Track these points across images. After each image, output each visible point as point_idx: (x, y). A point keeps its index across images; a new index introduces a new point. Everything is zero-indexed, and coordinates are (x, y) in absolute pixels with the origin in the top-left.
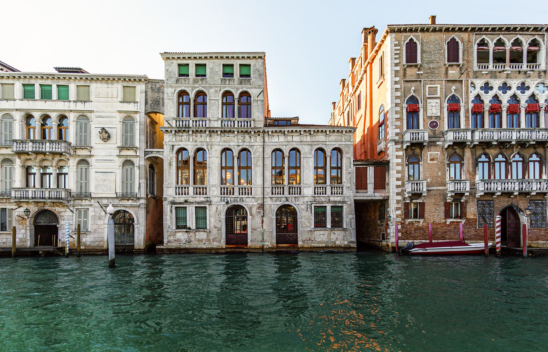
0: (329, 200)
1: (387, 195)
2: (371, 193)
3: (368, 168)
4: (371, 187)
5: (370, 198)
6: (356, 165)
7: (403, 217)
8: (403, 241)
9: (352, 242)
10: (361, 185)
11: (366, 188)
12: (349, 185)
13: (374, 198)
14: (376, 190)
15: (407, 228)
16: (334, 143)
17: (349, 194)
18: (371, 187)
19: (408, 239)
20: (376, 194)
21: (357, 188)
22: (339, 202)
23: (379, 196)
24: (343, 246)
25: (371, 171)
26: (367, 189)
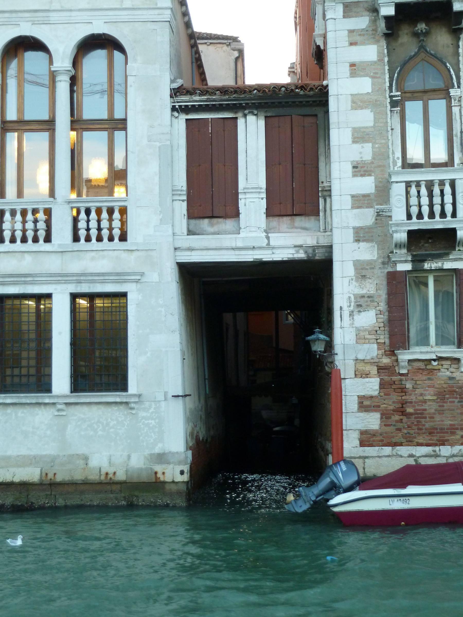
1: (324, 242)
3: (241, 122)
6: (186, 110)
8: (388, 450)
13: (267, 256)
14: (275, 222)
15: (403, 390)
19: (410, 441)
20: (277, 239)
21: (194, 213)
23: (285, 244)
24: (121, 476)
25: (252, 134)
26: (236, 215)
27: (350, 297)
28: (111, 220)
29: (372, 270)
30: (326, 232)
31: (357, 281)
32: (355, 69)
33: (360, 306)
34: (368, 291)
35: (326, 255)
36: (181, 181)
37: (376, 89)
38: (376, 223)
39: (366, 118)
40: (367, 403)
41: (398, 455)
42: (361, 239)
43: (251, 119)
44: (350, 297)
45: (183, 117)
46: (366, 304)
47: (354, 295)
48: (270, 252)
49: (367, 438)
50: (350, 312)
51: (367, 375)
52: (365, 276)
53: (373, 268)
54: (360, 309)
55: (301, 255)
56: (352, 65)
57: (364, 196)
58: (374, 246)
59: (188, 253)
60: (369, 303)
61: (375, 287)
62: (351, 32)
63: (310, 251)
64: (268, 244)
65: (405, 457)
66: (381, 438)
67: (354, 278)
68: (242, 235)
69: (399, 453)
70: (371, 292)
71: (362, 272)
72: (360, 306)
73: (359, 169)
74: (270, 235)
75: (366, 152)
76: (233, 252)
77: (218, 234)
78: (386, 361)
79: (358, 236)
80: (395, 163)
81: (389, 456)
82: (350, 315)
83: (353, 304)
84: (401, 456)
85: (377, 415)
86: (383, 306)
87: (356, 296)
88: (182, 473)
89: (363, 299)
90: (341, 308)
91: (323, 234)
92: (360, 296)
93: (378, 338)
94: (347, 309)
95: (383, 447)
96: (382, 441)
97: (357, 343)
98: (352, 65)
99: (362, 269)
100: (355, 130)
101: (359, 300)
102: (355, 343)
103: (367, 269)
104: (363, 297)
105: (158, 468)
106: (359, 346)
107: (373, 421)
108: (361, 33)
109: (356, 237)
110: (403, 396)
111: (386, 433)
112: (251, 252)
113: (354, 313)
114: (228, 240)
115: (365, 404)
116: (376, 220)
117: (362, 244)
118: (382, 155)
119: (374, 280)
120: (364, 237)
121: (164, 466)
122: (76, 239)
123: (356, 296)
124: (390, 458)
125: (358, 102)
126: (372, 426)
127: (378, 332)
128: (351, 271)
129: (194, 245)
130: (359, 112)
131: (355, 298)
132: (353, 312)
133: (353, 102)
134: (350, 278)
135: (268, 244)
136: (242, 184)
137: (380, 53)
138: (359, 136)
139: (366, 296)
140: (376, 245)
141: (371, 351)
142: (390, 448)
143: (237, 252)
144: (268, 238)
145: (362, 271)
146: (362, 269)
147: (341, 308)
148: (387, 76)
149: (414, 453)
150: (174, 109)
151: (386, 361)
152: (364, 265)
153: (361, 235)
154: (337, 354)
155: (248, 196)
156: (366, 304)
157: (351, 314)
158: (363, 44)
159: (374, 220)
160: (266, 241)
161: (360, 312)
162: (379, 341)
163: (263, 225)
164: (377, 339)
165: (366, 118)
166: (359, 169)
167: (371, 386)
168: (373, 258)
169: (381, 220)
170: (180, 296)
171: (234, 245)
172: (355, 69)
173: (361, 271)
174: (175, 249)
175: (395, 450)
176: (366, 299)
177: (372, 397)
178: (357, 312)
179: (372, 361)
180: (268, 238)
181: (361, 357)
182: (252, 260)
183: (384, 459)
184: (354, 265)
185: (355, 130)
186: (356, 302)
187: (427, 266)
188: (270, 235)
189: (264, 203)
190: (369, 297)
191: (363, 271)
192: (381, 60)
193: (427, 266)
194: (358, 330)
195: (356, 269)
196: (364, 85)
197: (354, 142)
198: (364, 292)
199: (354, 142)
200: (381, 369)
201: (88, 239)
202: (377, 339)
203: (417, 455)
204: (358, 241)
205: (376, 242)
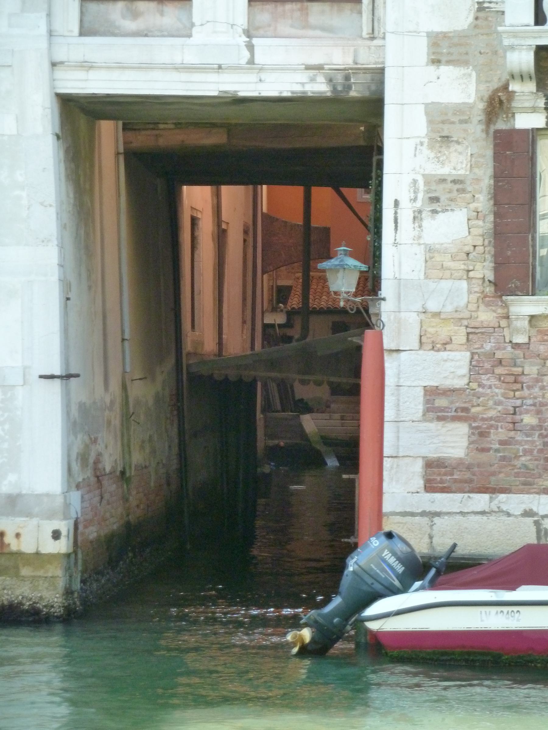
1: (368, 59)
5: (208, 86)
7: (485, 270)
8: (481, 501)
13: (247, 86)
20: (268, 50)
27: (415, 182)
29: (464, 126)
30: (373, 38)
31: (431, 147)
33: (435, 200)
34: (455, 169)
35: (373, 88)
38: (476, 26)
40: (442, 402)
41: (503, 511)
42: (444, 59)
44: (415, 182)
46: (448, 196)
47: (423, 175)
48: (252, 77)
49: (439, 476)
50: (414, 212)
51: (446, 345)
52: (447, 137)
53: (466, 122)
54: (435, 206)
55: (320, 87)
58: (470, 75)
59: (81, 74)
60: (455, 194)
61: (470, 160)
63: (339, 78)
64: (251, 62)
65: (516, 516)
66: (468, 475)
67: (426, 140)
69: (504, 508)
70: (460, 172)
71: (443, 129)
72: (435, 200)
74: (255, 41)
76: (175, 76)
77: (146, 35)
78: (486, 316)
79: (438, 53)
81: (483, 513)
82: (414, 218)
83: (420, 196)
84: (509, 515)
86: (483, 202)
87: (428, 179)
88: (56, 535)
89: (442, 186)
90: (397, 203)
91: (368, 43)
92: (439, 177)
93: (471, 268)
94: (410, 205)
95: (471, 495)
96: (471, 481)
97: (427, 277)
99: (443, 122)
101: (433, 188)
102: (422, 276)
103: (453, 123)
104: (443, 180)
106: (432, 285)
107: (453, 442)
109: (434, 53)
110: (518, 390)
111: (479, 465)
112: (213, 77)
113: (424, 215)
114: (165, 50)
115: (440, 404)
116: (477, 18)
117: (444, 69)
119: (467, 147)
120: (449, 53)
121: (20, 520)
123: (428, 179)
124: (485, 518)
126: (452, 451)
127: (471, 256)
128: (419, 126)
129: (93, 57)
131: (427, 183)
132: (420, 212)
134: (418, 141)
135: (251, 62)
139: (450, 179)
140: (474, 74)
141: (456, 294)
142: (486, 496)
143: (184, 76)
144: (250, 47)
145: (442, 128)
146: (443, 122)
147: (397, 203)
149: (535, 509)
151: (486, 316)
152: (446, 114)
153: (444, 50)
154: (384, 299)
156: (448, 196)
157: (417, 217)
159: (471, 18)
160: (246, 54)
161: (435, 212)
162: (471, 274)
163: (242, 20)
164: (468, 271)
167: (452, 368)
168: (467, 101)
169: (486, 19)
170: (62, 165)
171: (178, 60)
173: (441, 125)
174: (54, 65)
175: (496, 502)
176: (449, 186)
177: (453, 391)
178: (430, 213)
179: (457, 315)
180: (250, 47)
181: (433, 306)
182: (215, 94)
183: (472, 518)
184: (427, 114)
186: (427, 192)
188: (255, 41)
190: (454, 182)
191: (446, 127)
194: (431, 251)
195: (430, 122)
198: (445, 170)
200: (473, 333)
202: (468, 271)
203: (541, 513)
204: (436, 62)
205: (475, 67)
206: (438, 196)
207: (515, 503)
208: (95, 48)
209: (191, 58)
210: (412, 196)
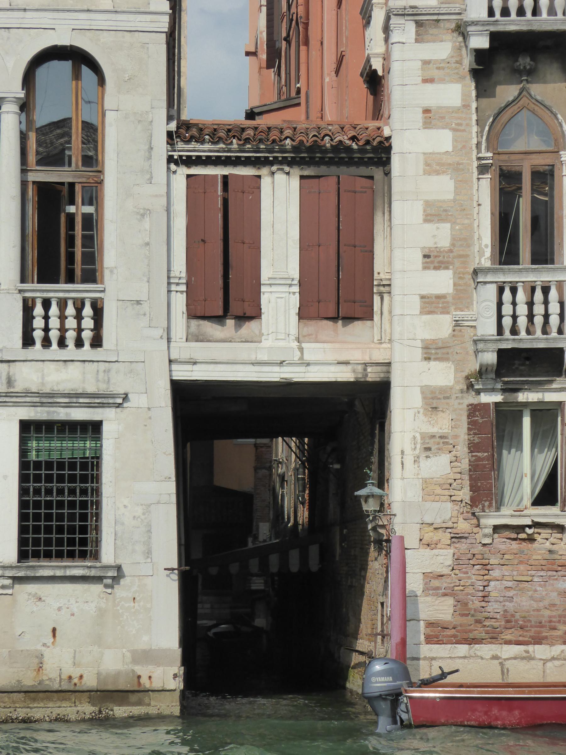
0: (10, 382)
1: (379, 356)
2: (280, 348)
3: (266, 182)
4: (280, 301)
5: (273, 375)
6: (189, 162)
8: (463, 649)
9: (146, 656)
10: (223, 289)
11: (250, 314)
12: (140, 290)
14: (312, 327)
16: (46, 19)
17: (143, 350)
18: (280, 301)
20: (313, 351)
22: (74, 398)
25: (280, 199)
27: (414, 438)
28: (79, 317)
29: (448, 401)
30: (381, 343)
31: (425, 415)
32: (430, 117)
33: (429, 449)
34: (441, 429)
35: (382, 375)
36: (180, 266)
37: (460, 146)
38: (454, 336)
39: (443, 187)
41: (478, 656)
42: (432, 357)
43: (280, 177)
44: (414, 438)
45: (183, 171)
46: (437, 446)
47: (420, 433)
48: (302, 369)
50: (414, 457)
52: (436, 408)
53: (448, 398)
54: (428, 453)
56: (427, 111)
57: (438, 297)
58: (450, 367)
59: (189, 367)
60: (441, 445)
61: (452, 423)
62: (426, 63)
64: (302, 358)
65: (487, 659)
66: (453, 632)
67: (422, 411)
68: (266, 343)
69: (479, 653)
70: (444, 431)
71: (433, 403)
72: (429, 449)
73: (432, 259)
74: (304, 345)
75: (441, 236)
76: (251, 368)
77: (230, 341)
78: (463, 526)
79: (429, 353)
80: (481, 253)
81: (465, 657)
82: (415, 461)
83: (418, 446)
84: (482, 658)
85: (450, 601)
89: (433, 440)
90: (403, 452)
91: (378, 346)
92: (431, 434)
93: (453, 494)
94: (411, 453)
95: (456, 645)
96: (455, 636)
97: (424, 500)
98: (427, 111)
99: (433, 398)
100: (428, 204)
101: (427, 441)
102: (421, 499)
103: (439, 399)
104: (433, 436)
105: (143, 671)
106: (428, 505)
108: (440, 65)
109: (426, 353)
110: (486, 575)
111: (461, 625)
112: (277, 369)
113: (421, 459)
116: (454, 331)
117: (432, 363)
118: (463, 240)
119: (449, 414)
120: (436, 353)
121: (150, 667)
122: (28, 341)
124: (466, 661)
125: (433, 165)
126: (443, 616)
127: (453, 487)
128: (417, 401)
129: (198, 356)
130: (435, 178)
131: (423, 438)
132: (418, 457)
133: (427, 164)
134: (416, 410)
135: (302, 358)
136: (266, 273)
137: (465, 96)
138: (434, 213)
139: (438, 435)
140: (453, 367)
141: (444, 511)
142: (466, 646)
143: (257, 368)
144: (301, 350)
145: (433, 401)
146: (433, 398)
147: (403, 452)
148: (475, 129)
149: (499, 655)
150: (170, 160)
152: (435, 393)
153: (432, 351)
154: (395, 515)
155: (274, 289)
156: (437, 446)
157: (416, 461)
158: (442, 81)
159: (450, 331)
160: (298, 354)
161: (427, 457)
162: (453, 498)
164: (451, 496)
165: (443, 187)
166: (432, 259)
167: (442, 559)
168: (448, 384)
169: (460, 331)
171: (253, 358)
172: (430, 117)
173: (431, 400)
174: (170, 361)
175: (473, 650)
176: (438, 440)
178: (425, 458)
179: (444, 525)
180: (301, 350)
181: (428, 520)
182: (278, 380)
183: (458, 661)
184: (422, 393)
185: (428, 204)
186: (423, 443)
187: (522, 397)
188: (304, 345)
189: (295, 300)
190: (441, 437)
191: (435, 401)
192: (466, 106)
193: (522, 397)
195: (424, 398)
196: (442, 141)
197: (426, 221)
199: (426, 221)
201: (46, 343)
202: (451, 496)
203: (504, 657)
204: (428, 359)
205: (453, 362)
206: (429, 446)
207: (486, 650)
208: (197, 350)
209: (264, 357)
210: (413, 446)
